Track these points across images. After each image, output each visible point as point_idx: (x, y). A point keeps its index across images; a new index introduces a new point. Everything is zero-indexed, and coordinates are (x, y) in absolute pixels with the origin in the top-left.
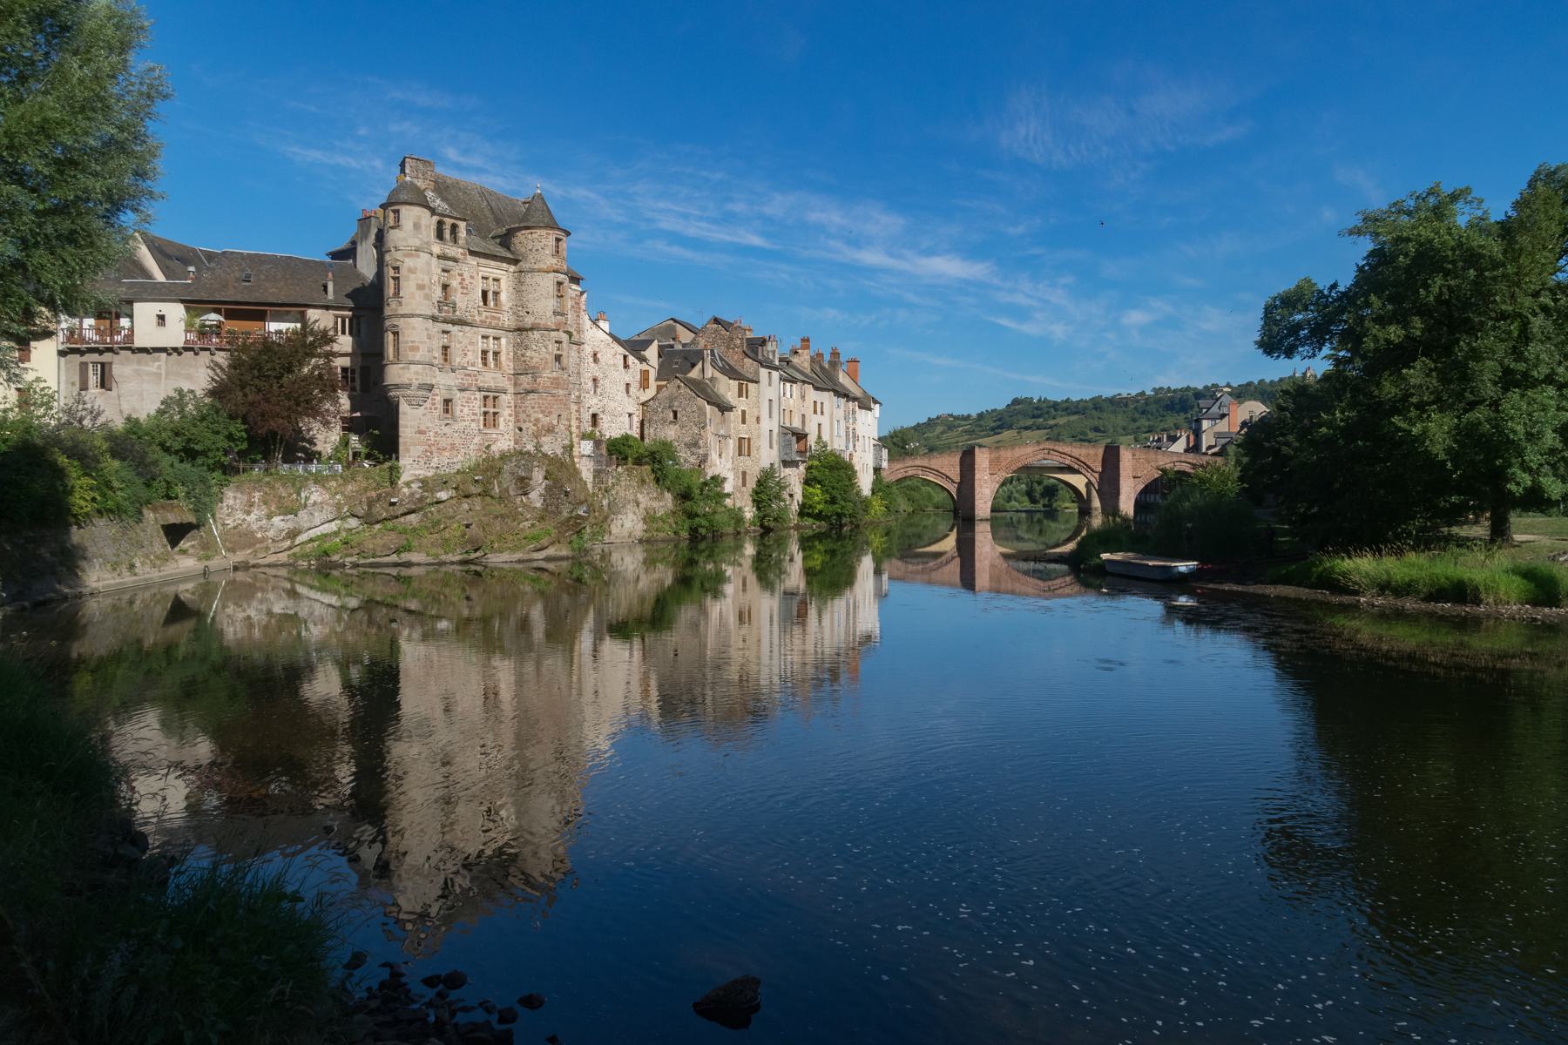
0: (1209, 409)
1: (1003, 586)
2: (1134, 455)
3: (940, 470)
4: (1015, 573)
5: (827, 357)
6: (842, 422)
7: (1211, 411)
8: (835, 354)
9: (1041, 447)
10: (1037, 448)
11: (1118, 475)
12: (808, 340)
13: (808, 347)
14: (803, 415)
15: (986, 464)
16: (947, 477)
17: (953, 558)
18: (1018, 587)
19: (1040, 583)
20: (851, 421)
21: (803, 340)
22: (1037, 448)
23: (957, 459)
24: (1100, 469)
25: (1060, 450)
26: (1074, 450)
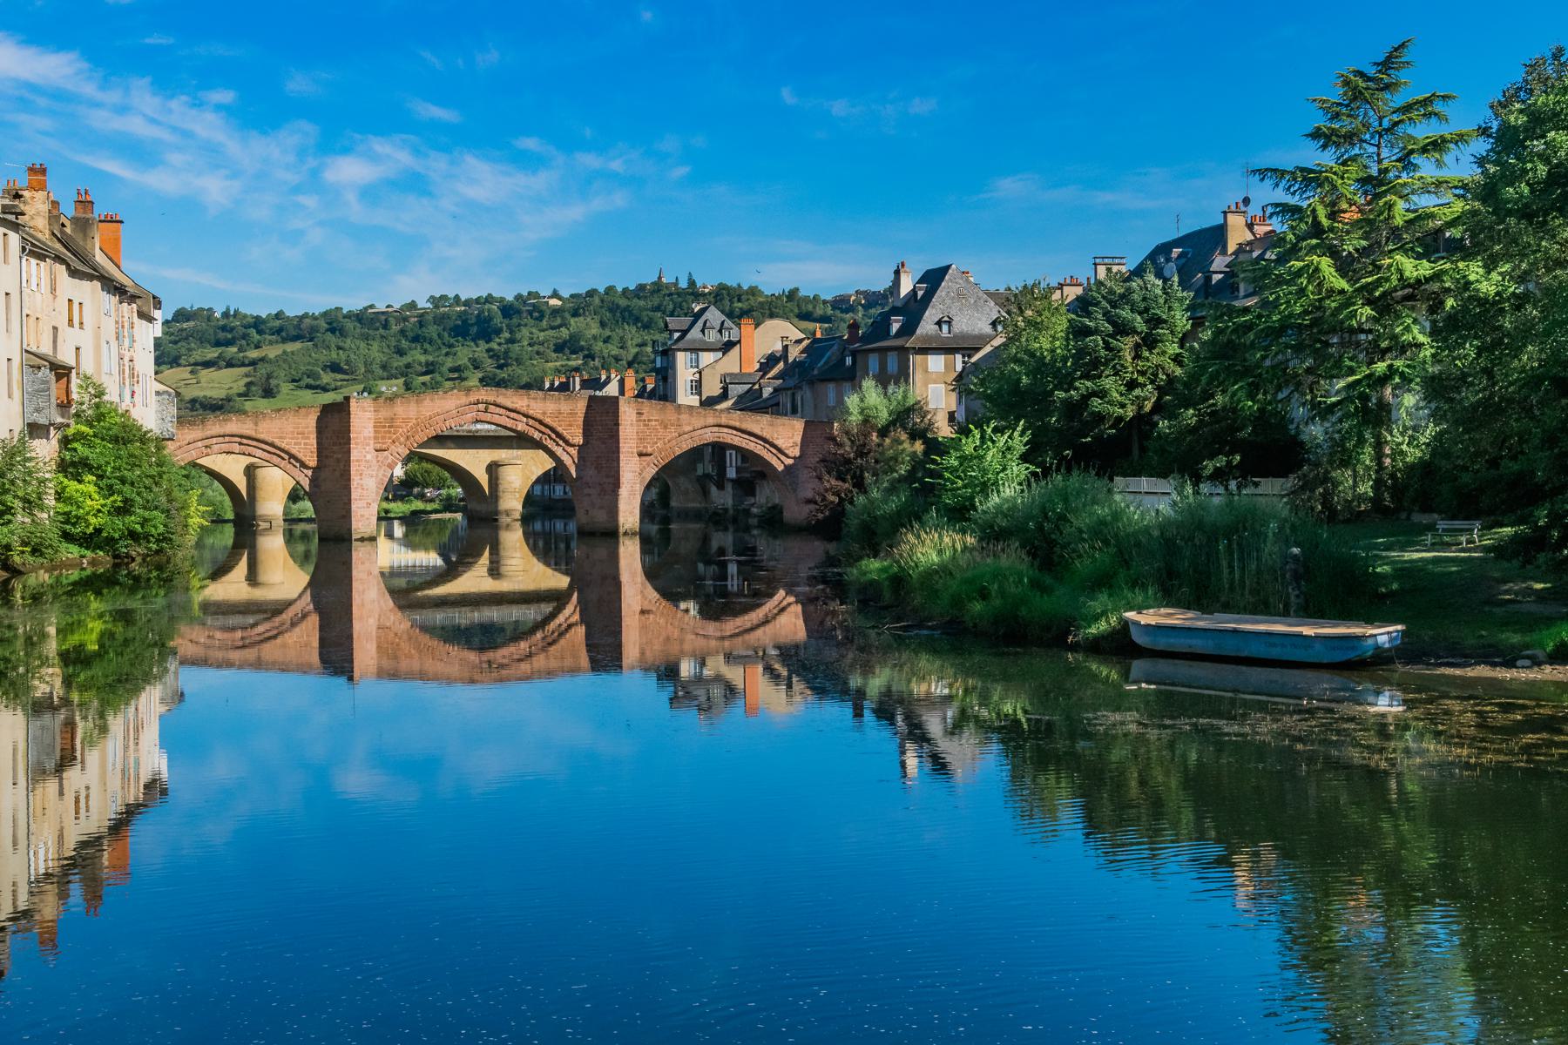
0: (685, 333)
1: (404, 665)
3: (277, 442)
4: (425, 639)
5: (69, 210)
6: (114, 344)
7: (689, 336)
8: (85, 203)
9: (473, 398)
10: (464, 400)
11: (617, 451)
12: (43, 171)
13: (42, 187)
14: (55, 329)
16: (292, 456)
17: (305, 616)
18: (431, 666)
19: (472, 656)
20: (127, 342)
21: (32, 170)
22: (464, 400)
23: (310, 421)
24: (579, 440)
25: (510, 405)
26: (533, 404)
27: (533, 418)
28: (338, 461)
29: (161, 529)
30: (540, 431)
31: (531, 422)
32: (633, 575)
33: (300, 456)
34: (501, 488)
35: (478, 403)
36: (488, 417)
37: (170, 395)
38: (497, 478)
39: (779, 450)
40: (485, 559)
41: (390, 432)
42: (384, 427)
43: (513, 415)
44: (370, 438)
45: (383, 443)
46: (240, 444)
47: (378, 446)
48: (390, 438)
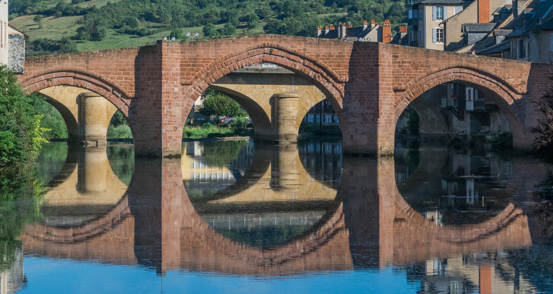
1: (202, 260)
2: (395, 57)
3: (104, 77)
4: (219, 238)
9: (260, 43)
10: (253, 44)
11: (376, 87)
15: (176, 69)
16: (115, 88)
17: (124, 218)
18: (224, 262)
19: (257, 253)
22: (253, 44)
23: (131, 60)
24: (345, 78)
25: (289, 48)
26: (309, 48)
27: (309, 60)
28: (152, 93)
29: (12, 145)
30: (314, 71)
31: (307, 63)
32: (389, 189)
33: (122, 88)
34: (282, 116)
35: (264, 47)
36: (272, 58)
37: (20, 38)
38: (278, 109)
39: (510, 87)
40: (268, 175)
41: (193, 70)
42: (189, 65)
43: (292, 57)
44: (177, 74)
45: (188, 79)
46: (75, 78)
47: (184, 81)
48: (193, 75)
